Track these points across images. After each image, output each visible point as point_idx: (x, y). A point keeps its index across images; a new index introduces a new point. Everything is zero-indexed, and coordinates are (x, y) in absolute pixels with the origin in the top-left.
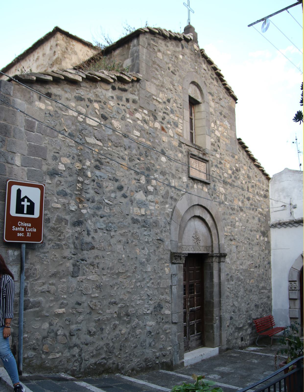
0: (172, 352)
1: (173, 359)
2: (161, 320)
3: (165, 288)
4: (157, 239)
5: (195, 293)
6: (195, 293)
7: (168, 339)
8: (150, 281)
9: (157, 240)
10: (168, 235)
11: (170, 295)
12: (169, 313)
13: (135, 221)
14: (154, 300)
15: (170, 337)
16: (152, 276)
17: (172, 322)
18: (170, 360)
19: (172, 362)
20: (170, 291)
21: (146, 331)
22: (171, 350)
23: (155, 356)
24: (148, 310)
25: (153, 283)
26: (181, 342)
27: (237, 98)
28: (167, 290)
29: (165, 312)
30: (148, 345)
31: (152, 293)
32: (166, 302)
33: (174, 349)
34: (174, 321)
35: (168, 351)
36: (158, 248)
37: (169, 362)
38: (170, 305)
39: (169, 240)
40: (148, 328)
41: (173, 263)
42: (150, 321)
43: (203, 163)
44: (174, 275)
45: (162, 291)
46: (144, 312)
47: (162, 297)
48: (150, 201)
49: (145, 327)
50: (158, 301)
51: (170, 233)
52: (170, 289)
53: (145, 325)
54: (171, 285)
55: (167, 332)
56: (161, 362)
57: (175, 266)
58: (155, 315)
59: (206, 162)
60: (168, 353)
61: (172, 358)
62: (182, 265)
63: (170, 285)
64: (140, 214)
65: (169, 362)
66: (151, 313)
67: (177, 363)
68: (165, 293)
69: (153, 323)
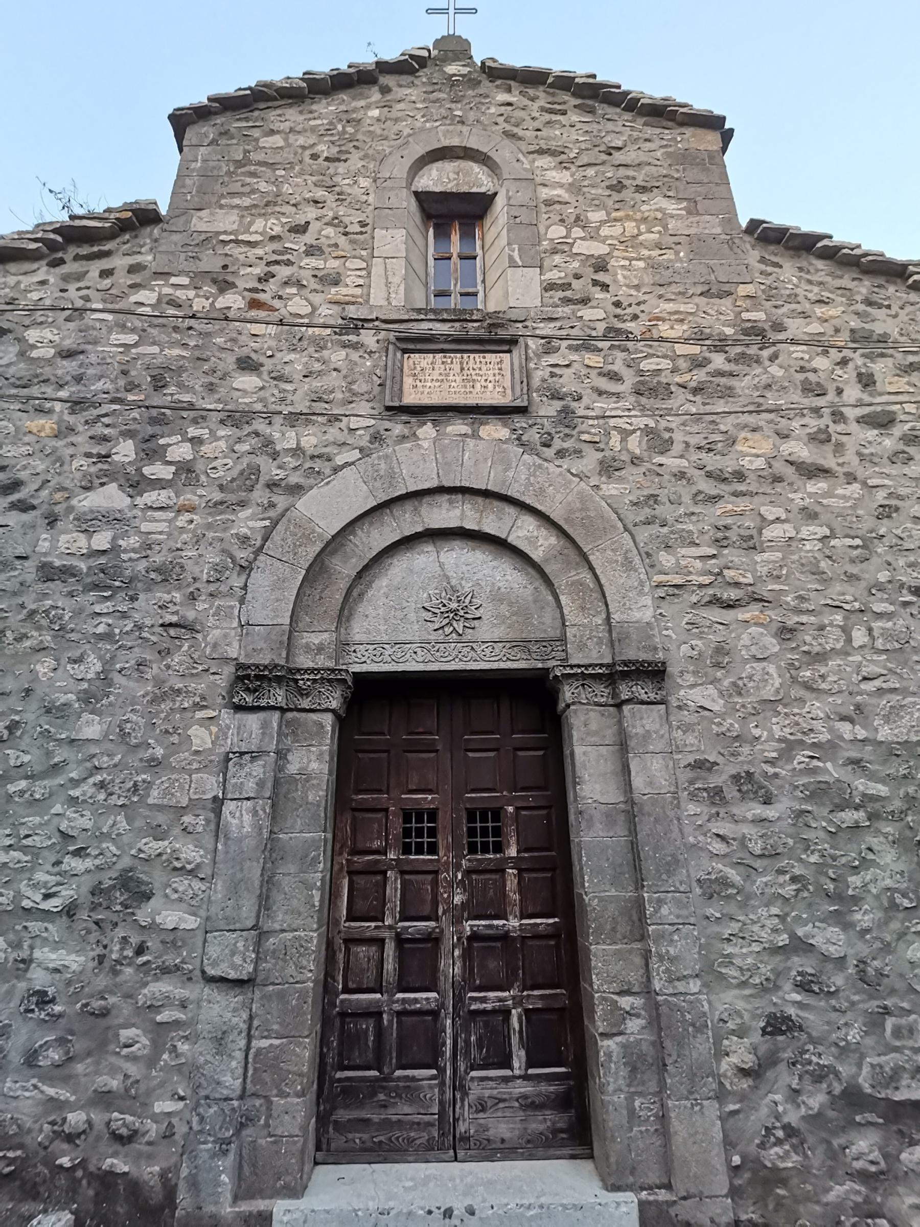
0: (181, 1129)
1: (184, 1172)
2: (129, 953)
3: (182, 810)
4: (161, 622)
5: (512, 852)
6: (512, 852)
7: (165, 1056)
8: (91, 775)
9: (162, 625)
10: (232, 607)
11: (208, 840)
12: (191, 922)
13: (48, 573)
14: (96, 857)
15: (183, 1047)
16: (105, 759)
17: (203, 972)
18: (163, 1175)
19: (170, 1193)
20: (208, 821)
21: (22, 986)
22: (175, 1121)
23: (53, 1123)
24: (47, 896)
25: (102, 785)
26: (282, 1095)
27: (717, 112)
28: (187, 819)
29: (158, 920)
30: (16, 1058)
31: (89, 825)
32: (175, 869)
33: (202, 1119)
34: (211, 972)
35: (155, 1118)
36: (165, 653)
37: (154, 1182)
38: (197, 885)
39: (235, 624)
40: (38, 978)
41: (239, 708)
42: (56, 946)
43: (488, 355)
44: (242, 754)
45: (161, 818)
46: (26, 903)
47: (153, 846)
48: (151, 507)
49: (26, 970)
50: (126, 862)
51: (242, 601)
52: (212, 815)
53: (23, 961)
54: (215, 798)
55: (159, 1018)
56: (92, 1168)
57: (253, 721)
58: (97, 923)
59: (506, 348)
60: (153, 1129)
61: (177, 1168)
62: (328, 720)
63: (209, 796)
64: (85, 551)
65: (154, 1182)
66: (70, 911)
67: (210, 1209)
68: (177, 831)
69: (73, 957)
